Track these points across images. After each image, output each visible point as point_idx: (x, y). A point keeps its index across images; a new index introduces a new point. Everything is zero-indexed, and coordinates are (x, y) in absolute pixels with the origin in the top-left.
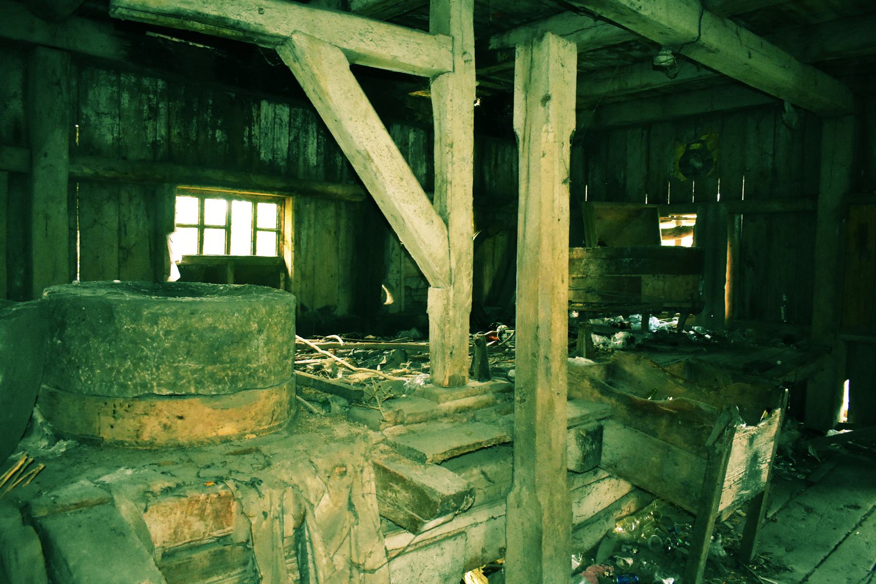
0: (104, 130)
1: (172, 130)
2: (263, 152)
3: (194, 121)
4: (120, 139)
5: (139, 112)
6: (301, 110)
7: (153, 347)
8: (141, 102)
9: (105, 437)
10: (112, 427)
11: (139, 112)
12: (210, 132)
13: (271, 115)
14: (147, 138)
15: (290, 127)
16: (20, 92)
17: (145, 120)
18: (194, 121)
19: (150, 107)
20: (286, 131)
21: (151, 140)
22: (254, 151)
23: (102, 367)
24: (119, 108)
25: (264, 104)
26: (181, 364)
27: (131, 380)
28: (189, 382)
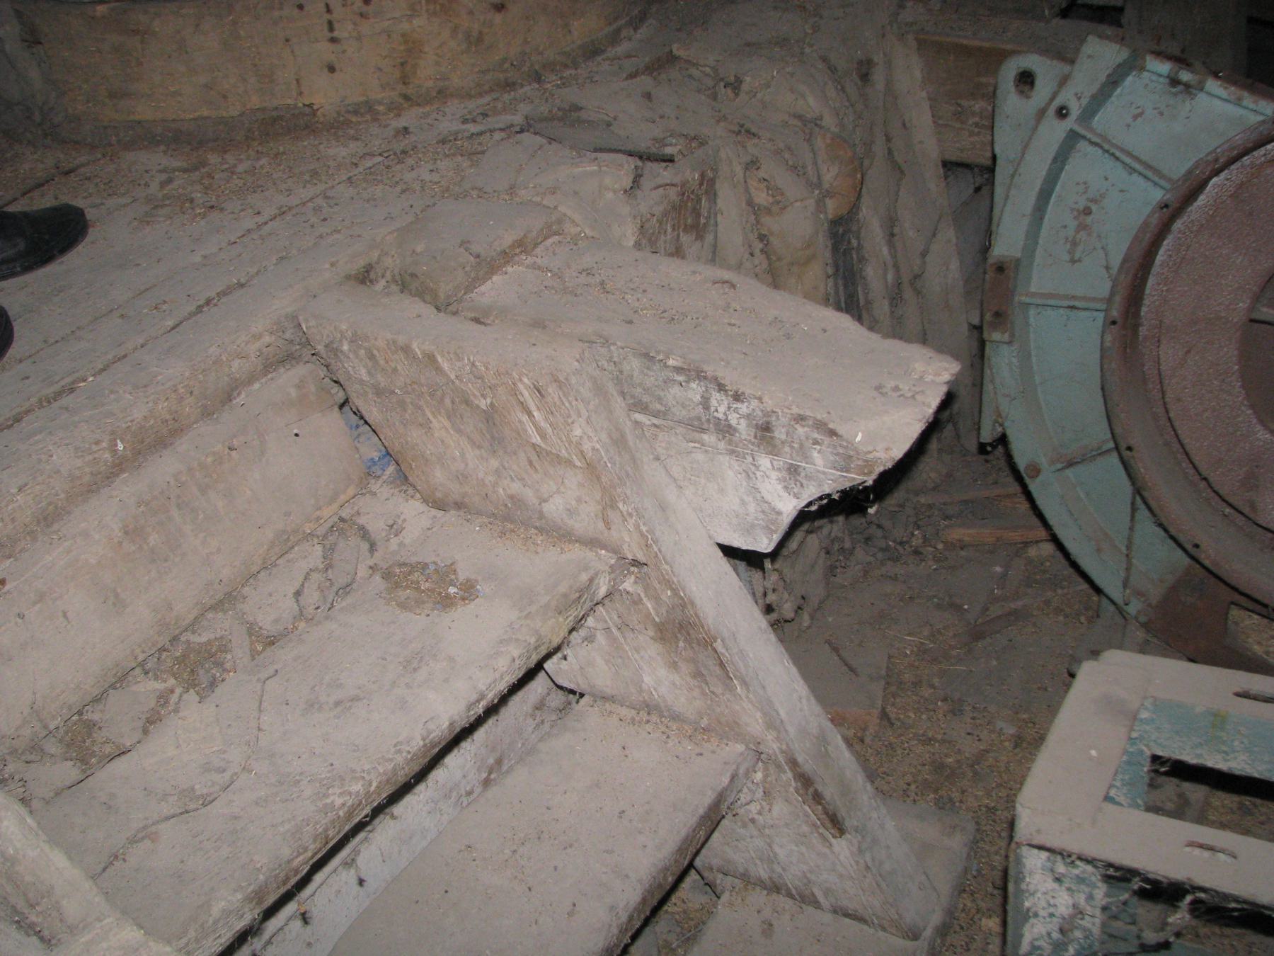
9: (318, 100)
10: (332, 69)
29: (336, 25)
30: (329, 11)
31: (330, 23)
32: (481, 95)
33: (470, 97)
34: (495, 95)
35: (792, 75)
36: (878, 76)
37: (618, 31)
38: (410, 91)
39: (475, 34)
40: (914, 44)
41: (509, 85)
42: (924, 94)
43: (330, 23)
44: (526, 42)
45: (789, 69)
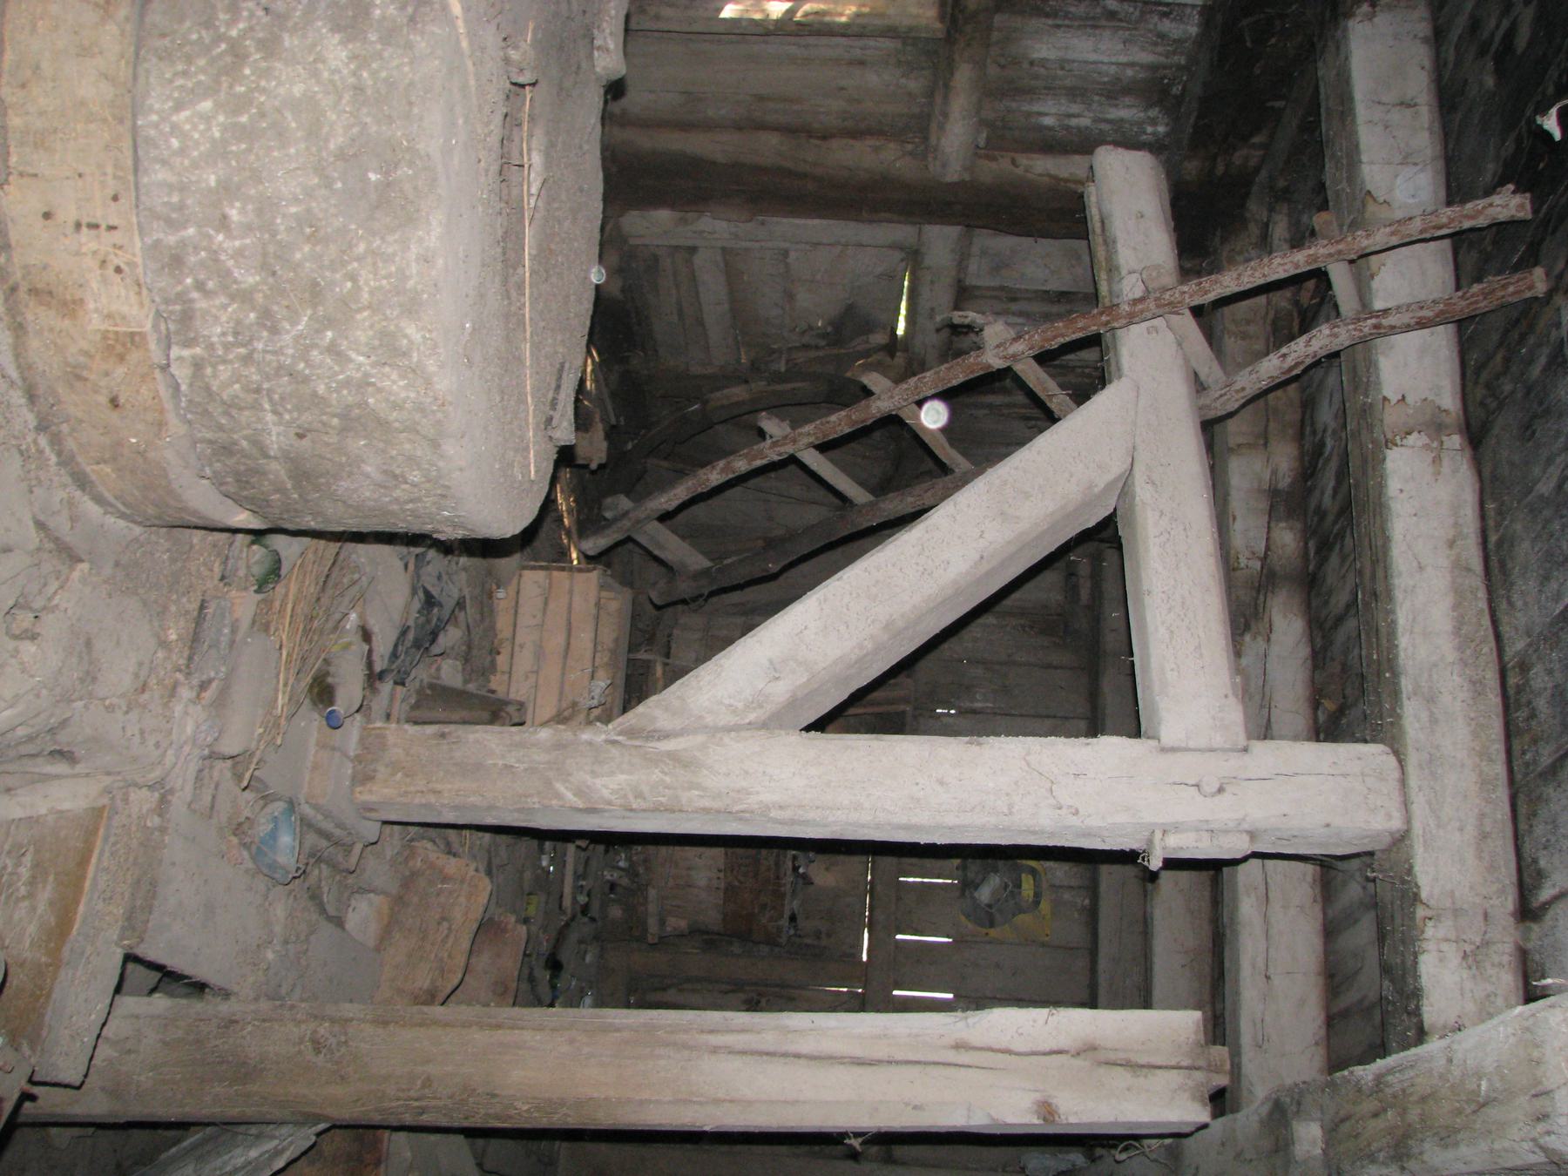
6: (1193, 30)
7: (308, 349)
10: (47, 216)
23: (227, 190)
26: (270, 417)
27: (200, 286)
28: (221, 428)
29: (93, 232)
30: (112, 228)
31: (97, 226)
32: (19, 367)
33: (17, 356)
34: (19, 382)
35: (38, 696)
36: (61, 768)
37: (111, 505)
38: (22, 294)
39: (85, 373)
40: (100, 803)
41: (32, 397)
42: (43, 811)
43: (97, 226)
44: (82, 421)
45: (44, 692)
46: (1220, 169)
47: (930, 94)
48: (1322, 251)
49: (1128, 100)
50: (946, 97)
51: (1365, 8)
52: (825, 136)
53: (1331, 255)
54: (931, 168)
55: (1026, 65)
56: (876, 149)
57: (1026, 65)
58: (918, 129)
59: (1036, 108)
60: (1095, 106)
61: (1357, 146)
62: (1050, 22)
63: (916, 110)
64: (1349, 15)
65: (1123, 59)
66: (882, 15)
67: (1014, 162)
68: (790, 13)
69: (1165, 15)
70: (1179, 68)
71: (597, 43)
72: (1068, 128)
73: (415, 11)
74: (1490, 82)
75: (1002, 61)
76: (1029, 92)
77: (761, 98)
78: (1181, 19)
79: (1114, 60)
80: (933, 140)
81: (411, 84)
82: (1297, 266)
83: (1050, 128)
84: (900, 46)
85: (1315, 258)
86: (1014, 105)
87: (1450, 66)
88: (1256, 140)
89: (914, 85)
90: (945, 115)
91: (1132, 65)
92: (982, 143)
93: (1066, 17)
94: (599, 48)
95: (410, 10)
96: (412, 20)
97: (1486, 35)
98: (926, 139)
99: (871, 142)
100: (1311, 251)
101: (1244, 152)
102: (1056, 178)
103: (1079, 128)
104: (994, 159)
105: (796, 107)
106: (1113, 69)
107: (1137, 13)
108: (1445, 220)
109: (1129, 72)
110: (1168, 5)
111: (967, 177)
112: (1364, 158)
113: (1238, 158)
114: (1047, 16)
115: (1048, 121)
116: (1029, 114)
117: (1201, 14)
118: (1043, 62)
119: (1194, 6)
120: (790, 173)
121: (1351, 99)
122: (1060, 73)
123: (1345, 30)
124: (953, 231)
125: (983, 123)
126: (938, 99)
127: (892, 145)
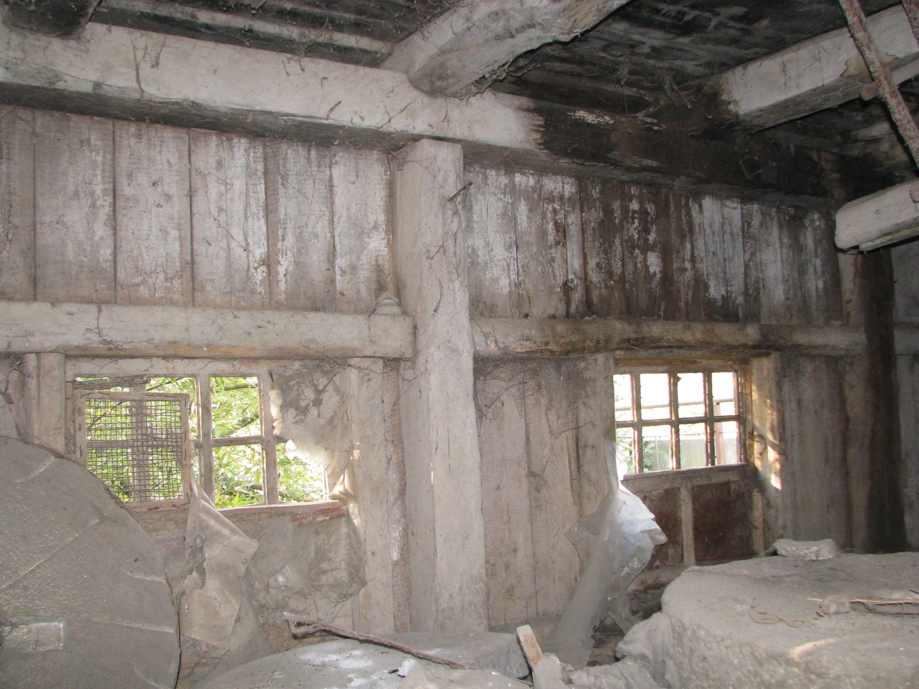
0: (496, 272)
1: (589, 260)
2: (712, 283)
3: (617, 241)
4: (520, 284)
5: (543, 234)
6: (756, 207)
8: (544, 217)
11: (543, 234)
12: (640, 258)
13: (717, 218)
14: (555, 277)
15: (744, 237)
16: (382, 218)
17: (551, 247)
18: (617, 241)
19: (556, 224)
20: (739, 245)
21: (560, 280)
22: (700, 284)
24: (515, 233)
25: (707, 202)
46: (835, 176)
47: (813, 357)
48: (887, 90)
49: (802, 239)
50: (817, 347)
51: (731, 107)
52: (846, 420)
53: (889, 84)
54: (859, 352)
55: (789, 302)
56: (852, 387)
57: (789, 302)
58: (834, 362)
59: (814, 293)
60: (807, 258)
61: (814, 90)
62: (762, 291)
63: (824, 366)
64: (737, 115)
65: (778, 245)
66: (770, 391)
67: (849, 302)
68: (774, 447)
69: (749, 224)
70: (778, 211)
71: (814, 558)
72: (823, 272)
73: (813, 673)
74: (765, 22)
75: (789, 316)
76: (804, 298)
77: (827, 460)
78: (750, 215)
79: (779, 251)
80: (842, 353)
81: (864, 677)
82: (899, 103)
83: (825, 282)
84: (786, 379)
85: (893, 94)
86: (813, 307)
87: (757, 50)
88: (815, 158)
89: (809, 367)
90: (826, 346)
91: (780, 239)
92: (840, 323)
93: (758, 282)
94: (817, 557)
95: (813, 677)
96: (820, 676)
97: (738, 33)
98: (841, 358)
99: (847, 392)
100: (888, 96)
101: (823, 163)
102: (855, 274)
103: (822, 266)
104: (848, 314)
105: (830, 439)
106: (785, 250)
107: (750, 241)
108: (856, 19)
109: (785, 240)
110: (743, 224)
111: (862, 329)
112: (820, 84)
113: (828, 167)
114: (758, 293)
115: (821, 285)
116: (818, 296)
117: (745, 204)
118: (786, 292)
119: (742, 209)
120: (873, 440)
121: (786, 101)
122: (790, 282)
123: (745, 115)
124: (898, 335)
125: (827, 323)
126: (815, 352)
127: (847, 378)
